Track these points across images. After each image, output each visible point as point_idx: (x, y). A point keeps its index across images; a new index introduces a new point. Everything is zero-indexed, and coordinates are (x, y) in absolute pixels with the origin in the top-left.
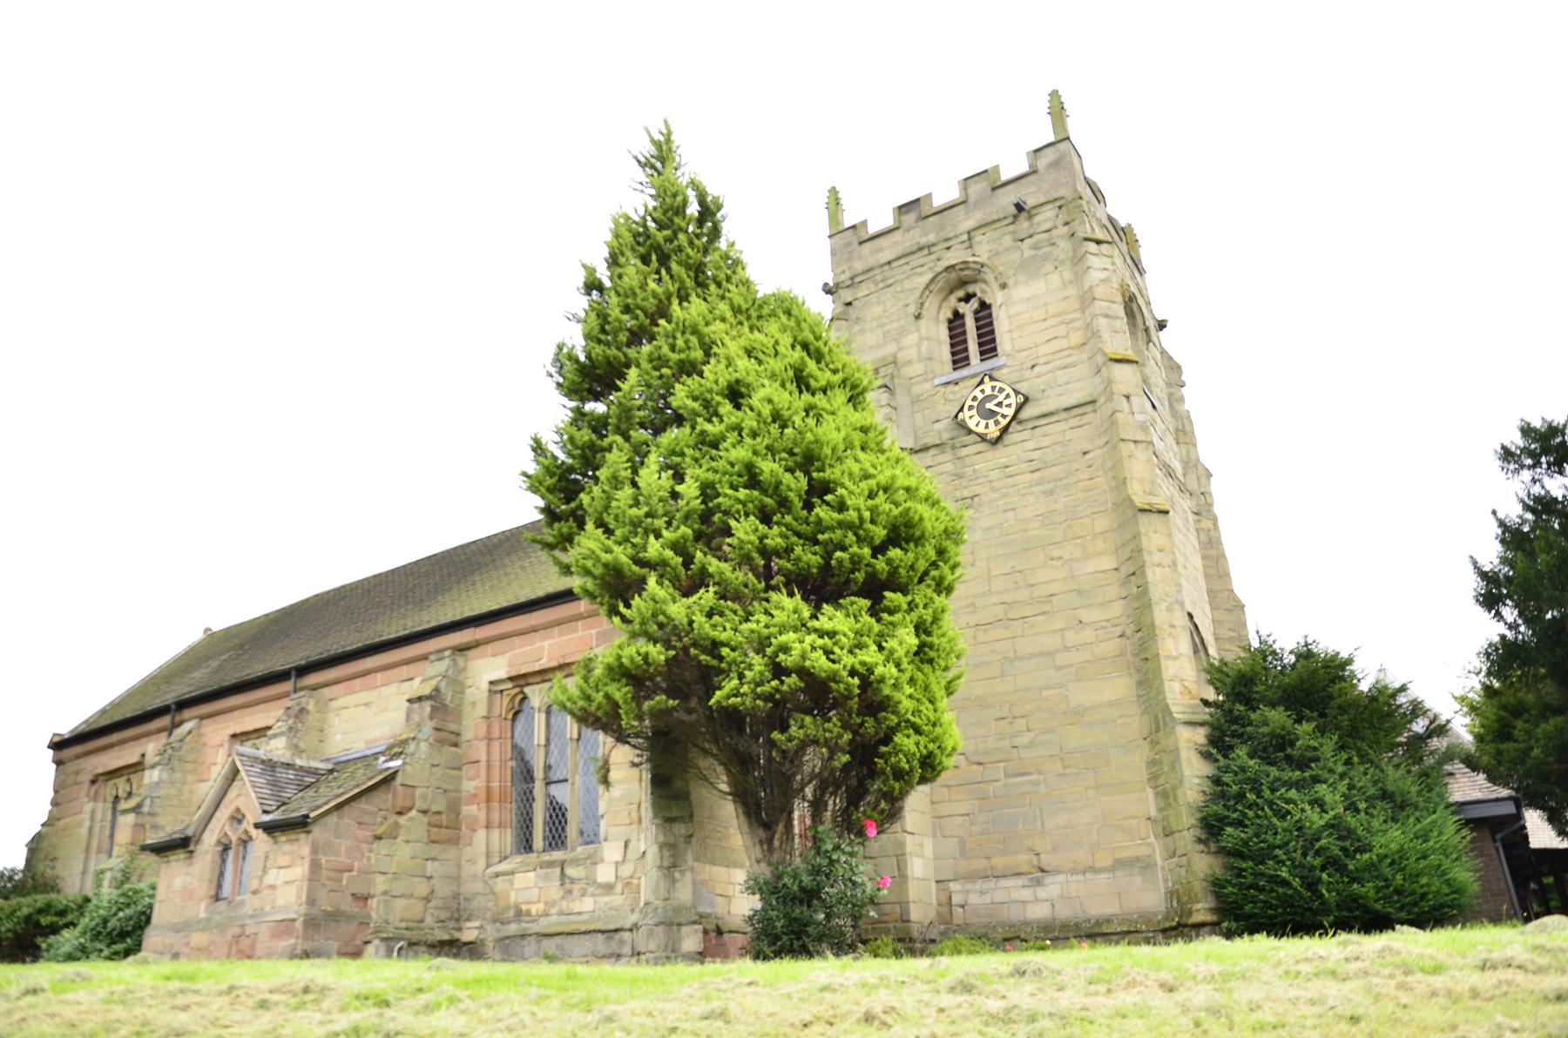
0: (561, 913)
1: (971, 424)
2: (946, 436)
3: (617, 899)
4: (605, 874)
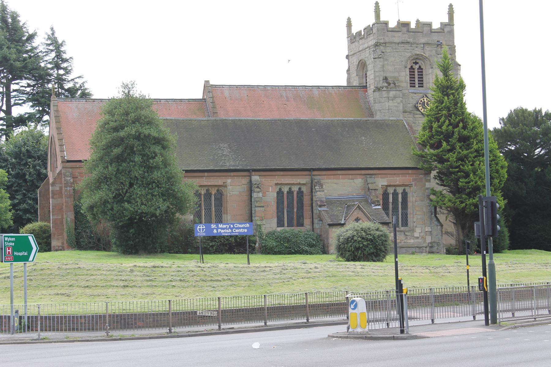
0: (405, 242)
1: (420, 108)
2: (411, 109)
3: (420, 240)
4: (416, 234)
